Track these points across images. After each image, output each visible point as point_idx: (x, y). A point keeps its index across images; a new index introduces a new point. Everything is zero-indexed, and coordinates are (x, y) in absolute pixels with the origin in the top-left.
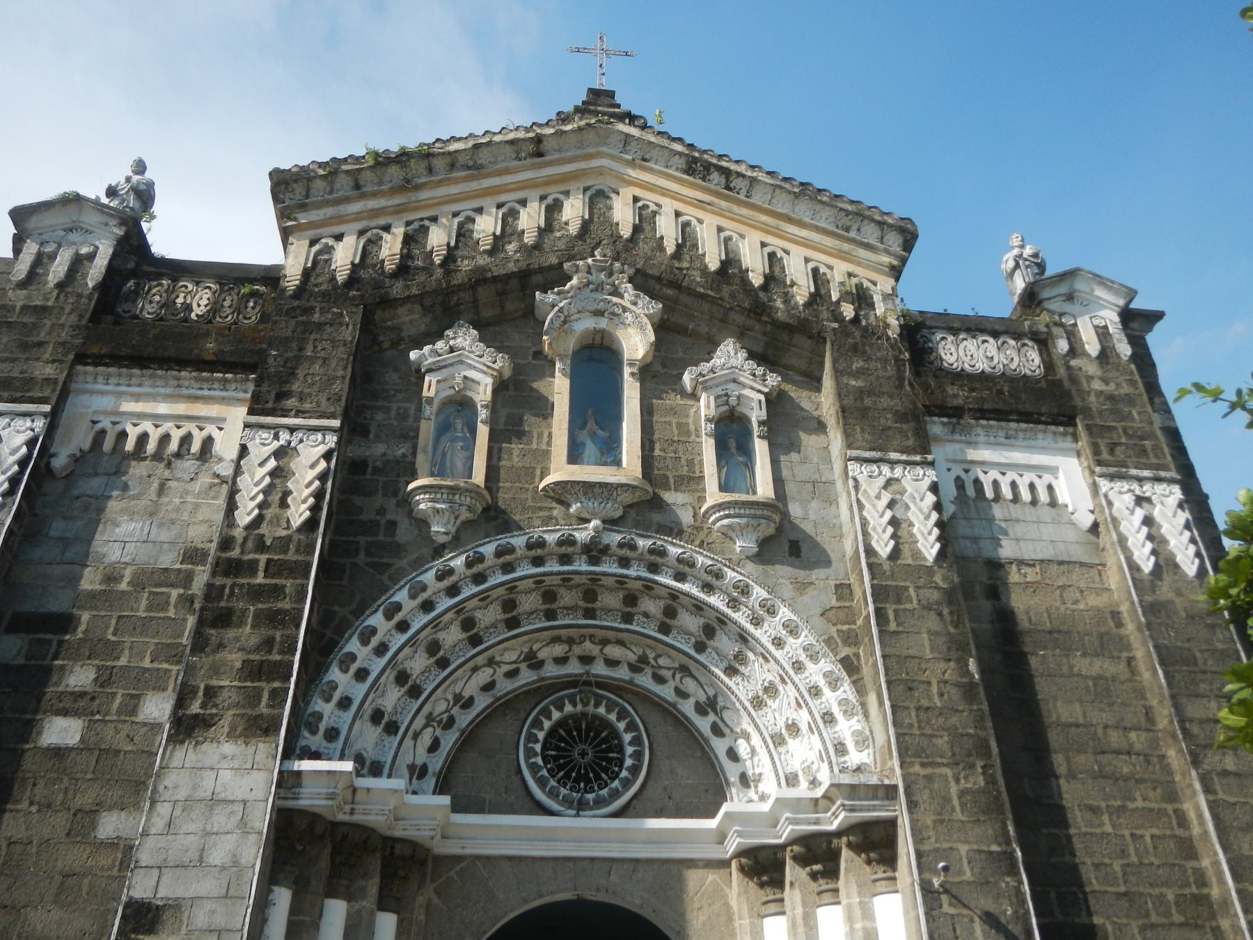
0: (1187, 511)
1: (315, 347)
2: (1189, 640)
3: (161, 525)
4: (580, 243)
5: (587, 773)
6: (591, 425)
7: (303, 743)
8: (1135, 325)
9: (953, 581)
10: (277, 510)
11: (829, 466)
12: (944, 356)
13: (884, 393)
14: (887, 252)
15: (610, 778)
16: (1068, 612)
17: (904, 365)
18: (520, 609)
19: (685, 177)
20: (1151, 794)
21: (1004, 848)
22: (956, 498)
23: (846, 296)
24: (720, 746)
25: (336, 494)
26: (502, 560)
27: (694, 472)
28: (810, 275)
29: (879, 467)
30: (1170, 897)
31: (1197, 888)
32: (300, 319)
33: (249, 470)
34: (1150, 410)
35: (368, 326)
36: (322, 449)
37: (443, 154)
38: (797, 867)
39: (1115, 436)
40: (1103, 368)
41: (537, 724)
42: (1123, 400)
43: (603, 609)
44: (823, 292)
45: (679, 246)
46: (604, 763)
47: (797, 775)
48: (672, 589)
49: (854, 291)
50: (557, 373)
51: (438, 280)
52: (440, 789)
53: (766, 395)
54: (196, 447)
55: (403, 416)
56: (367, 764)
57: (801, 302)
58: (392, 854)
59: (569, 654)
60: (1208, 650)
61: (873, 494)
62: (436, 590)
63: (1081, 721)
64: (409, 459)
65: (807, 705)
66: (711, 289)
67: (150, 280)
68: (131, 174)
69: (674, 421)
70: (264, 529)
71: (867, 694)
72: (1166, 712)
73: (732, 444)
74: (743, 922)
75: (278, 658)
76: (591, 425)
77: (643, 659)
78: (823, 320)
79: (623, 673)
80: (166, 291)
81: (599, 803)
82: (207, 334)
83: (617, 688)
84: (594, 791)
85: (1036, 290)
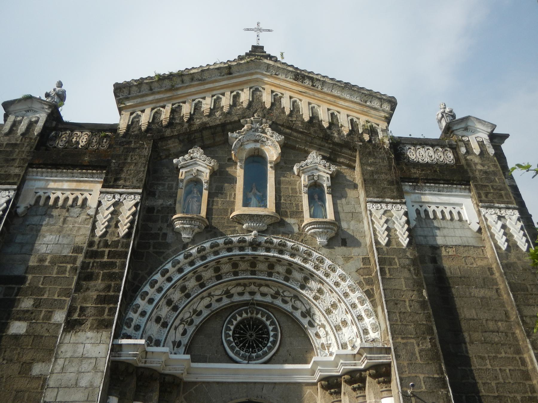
0: (522, 222)
1: (132, 158)
2: (524, 280)
3: (64, 237)
4: (248, 111)
5: (253, 344)
6: (254, 190)
7: (124, 331)
8: (496, 140)
9: (415, 255)
11: (359, 206)
12: (410, 156)
13: (382, 173)
14: (383, 111)
15: (263, 346)
16: (468, 268)
17: (392, 160)
18: (222, 271)
19: (294, 81)
20: (509, 350)
21: (440, 376)
22: (416, 219)
23: (365, 131)
24: (311, 332)
25: (140, 222)
26: (213, 249)
27: (299, 209)
28: (350, 122)
29: (381, 205)
30: (519, 398)
31: (531, 394)
32: (126, 146)
33: (102, 212)
34: (503, 177)
35: (155, 149)
36: (134, 202)
37: (188, 74)
38: (347, 385)
39: (488, 189)
40: (482, 159)
41: (230, 322)
42: (491, 173)
43: (259, 271)
44: (355, 129)
45: (291, 111)
47: (346, 344)
48: (289, 261)
49: (369, 129)
50: (238, 168)
51: (186, 129)
52: (186, 352)
53: (331, 175)
54: (80, 202)
55: (170, 187)
56: (154, 340)
59: (244, 291)
60: (533, 284)
61: (378, 217)
62: (184, 263)
63: (475, 317)
64: (173, 206)
66: (306, 130)
67: (61, 131)
68: (56, 87)
69: (290, 187)
70: (108, 237)
71: (377, 307)
72: (514, 313)
73: (316, 197)
75: (113, 294)
76: (254, 190)
77: (277, 293)
78: (355, 141)
79: (268, 299)
80: (68, 136)
81: (258, 357)
82: (85, 154)
83: (267, 306)
84: (256, 352)
85: (450, 126)
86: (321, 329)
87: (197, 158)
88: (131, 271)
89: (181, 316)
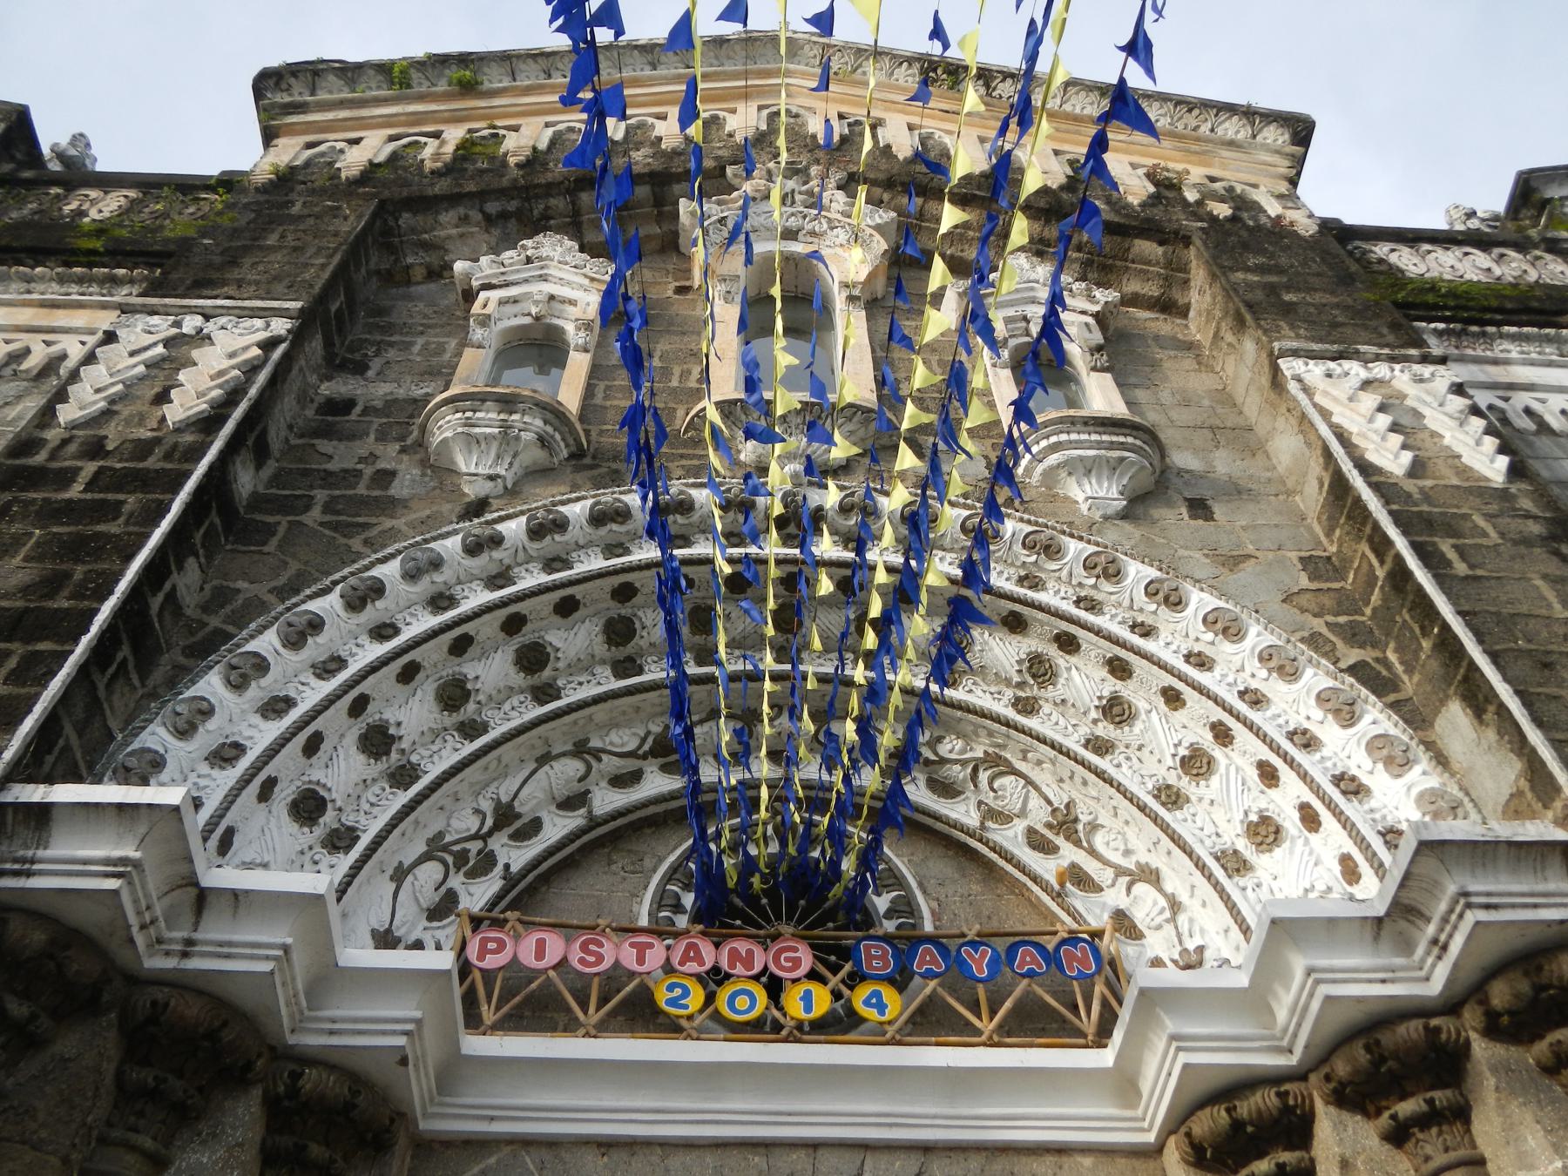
10: (146, 408)
13: (1316, 290)
26: (603, 531)
51: (515, 180)
53: (1096, 316)
54: (33, 362)
57: (1136, 202)
58: (293, 1092)
61: (1343, 397)
65: (1291, 763)
75: (66, 604)
85: (1534, 184)
86: (1141, 888)
87: (548, 258)
89: (430, 820)
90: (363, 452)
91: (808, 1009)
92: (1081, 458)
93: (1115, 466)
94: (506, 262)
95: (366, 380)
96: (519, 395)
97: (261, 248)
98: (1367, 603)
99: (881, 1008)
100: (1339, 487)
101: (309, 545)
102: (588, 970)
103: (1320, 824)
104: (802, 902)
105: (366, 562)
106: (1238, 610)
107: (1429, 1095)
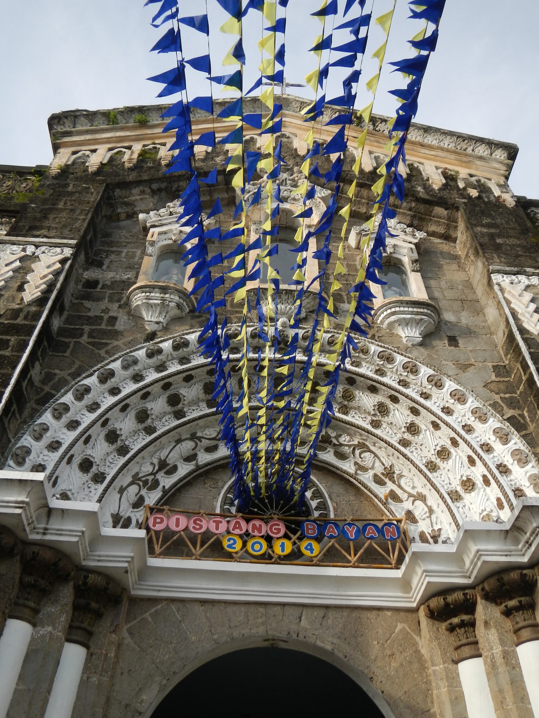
10: (14, 293)
13: (511, 237)
36: (60, 257)
46: (293, 526)
53: (416, 245)
57: (436, 188)
58: (85, 583)
61: (517, 294)
65: (481, 458)
66: (368, 181)
74: (437, 668)
86: (418, 503)
88: (37, 364)
89: (133, 468)
90: (103, 307)
91: (283, 550)
92: (404, 319)
93: (419, 322)
94: (161, 214)
95: (103, 270)
96: (168, 286)
97: (57, 209)
98: (518, 389)
99: (312, 550)
100: (511, 337)
101: (83, 353)
102: (196, 532)
103: (490, 484)
104: (282, 502)
105: (107, 362)
106: (464, 390)
107: (520, 599)
